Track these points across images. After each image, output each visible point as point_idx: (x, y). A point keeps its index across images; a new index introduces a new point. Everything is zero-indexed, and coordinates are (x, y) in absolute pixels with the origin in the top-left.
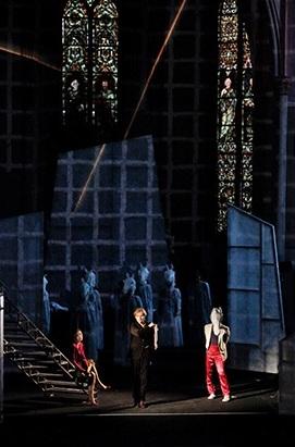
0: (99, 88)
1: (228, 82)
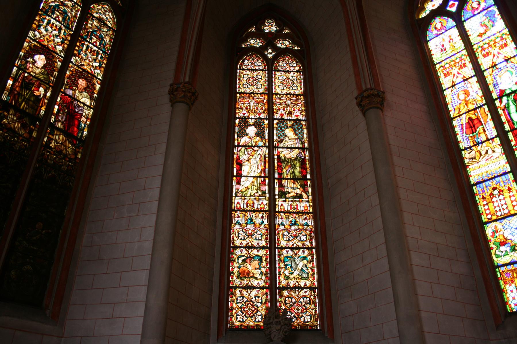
0: (73, 84)
1: (251, 131)
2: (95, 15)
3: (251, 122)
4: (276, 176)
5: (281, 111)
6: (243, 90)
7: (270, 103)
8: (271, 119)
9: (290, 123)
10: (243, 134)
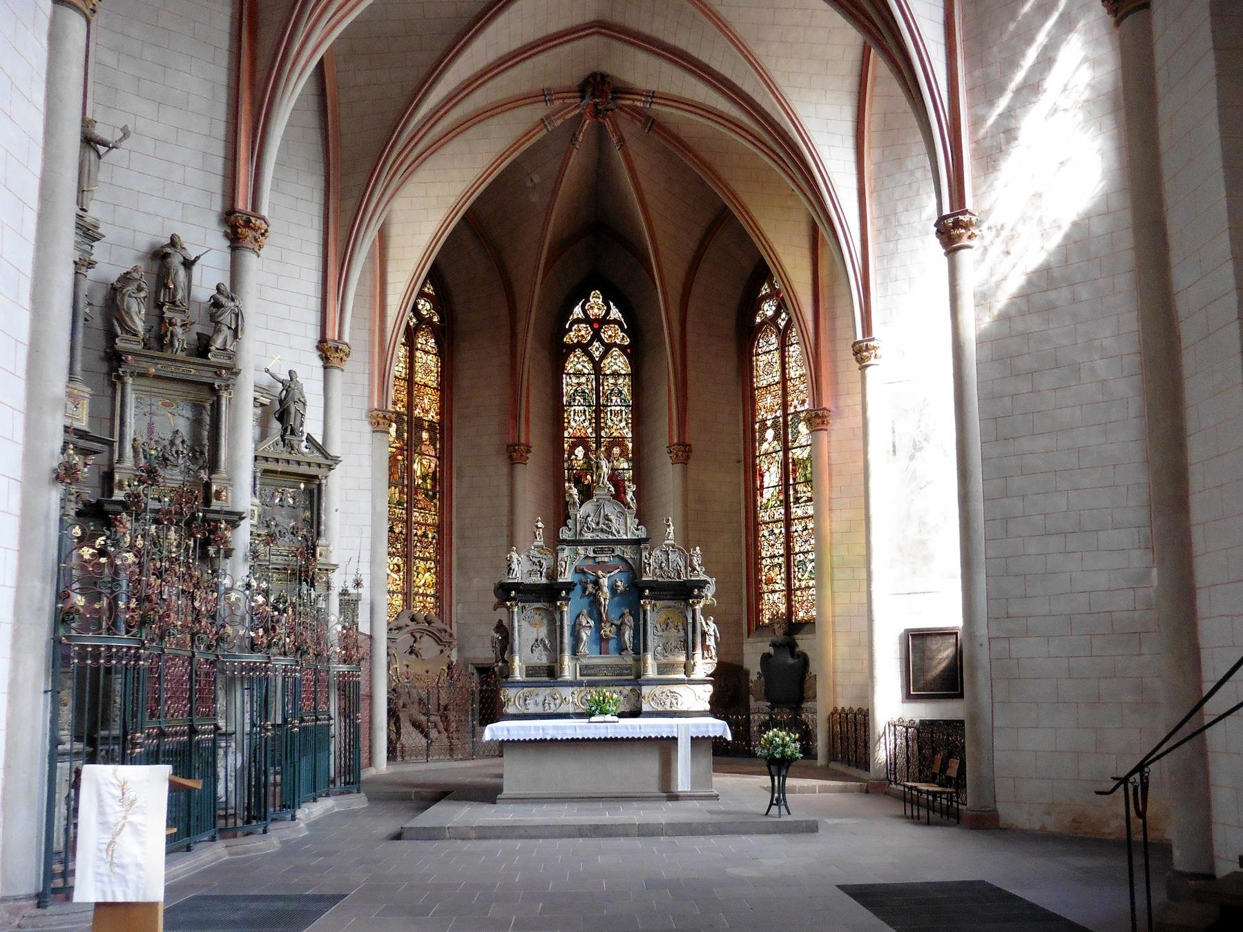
1: (770, 434)
2: (608, 372)
3: (769, 423)
4: (791, 482)
5: (796, 402)
8: (785, 415)
9: (802, 415)
10: (763, 440)
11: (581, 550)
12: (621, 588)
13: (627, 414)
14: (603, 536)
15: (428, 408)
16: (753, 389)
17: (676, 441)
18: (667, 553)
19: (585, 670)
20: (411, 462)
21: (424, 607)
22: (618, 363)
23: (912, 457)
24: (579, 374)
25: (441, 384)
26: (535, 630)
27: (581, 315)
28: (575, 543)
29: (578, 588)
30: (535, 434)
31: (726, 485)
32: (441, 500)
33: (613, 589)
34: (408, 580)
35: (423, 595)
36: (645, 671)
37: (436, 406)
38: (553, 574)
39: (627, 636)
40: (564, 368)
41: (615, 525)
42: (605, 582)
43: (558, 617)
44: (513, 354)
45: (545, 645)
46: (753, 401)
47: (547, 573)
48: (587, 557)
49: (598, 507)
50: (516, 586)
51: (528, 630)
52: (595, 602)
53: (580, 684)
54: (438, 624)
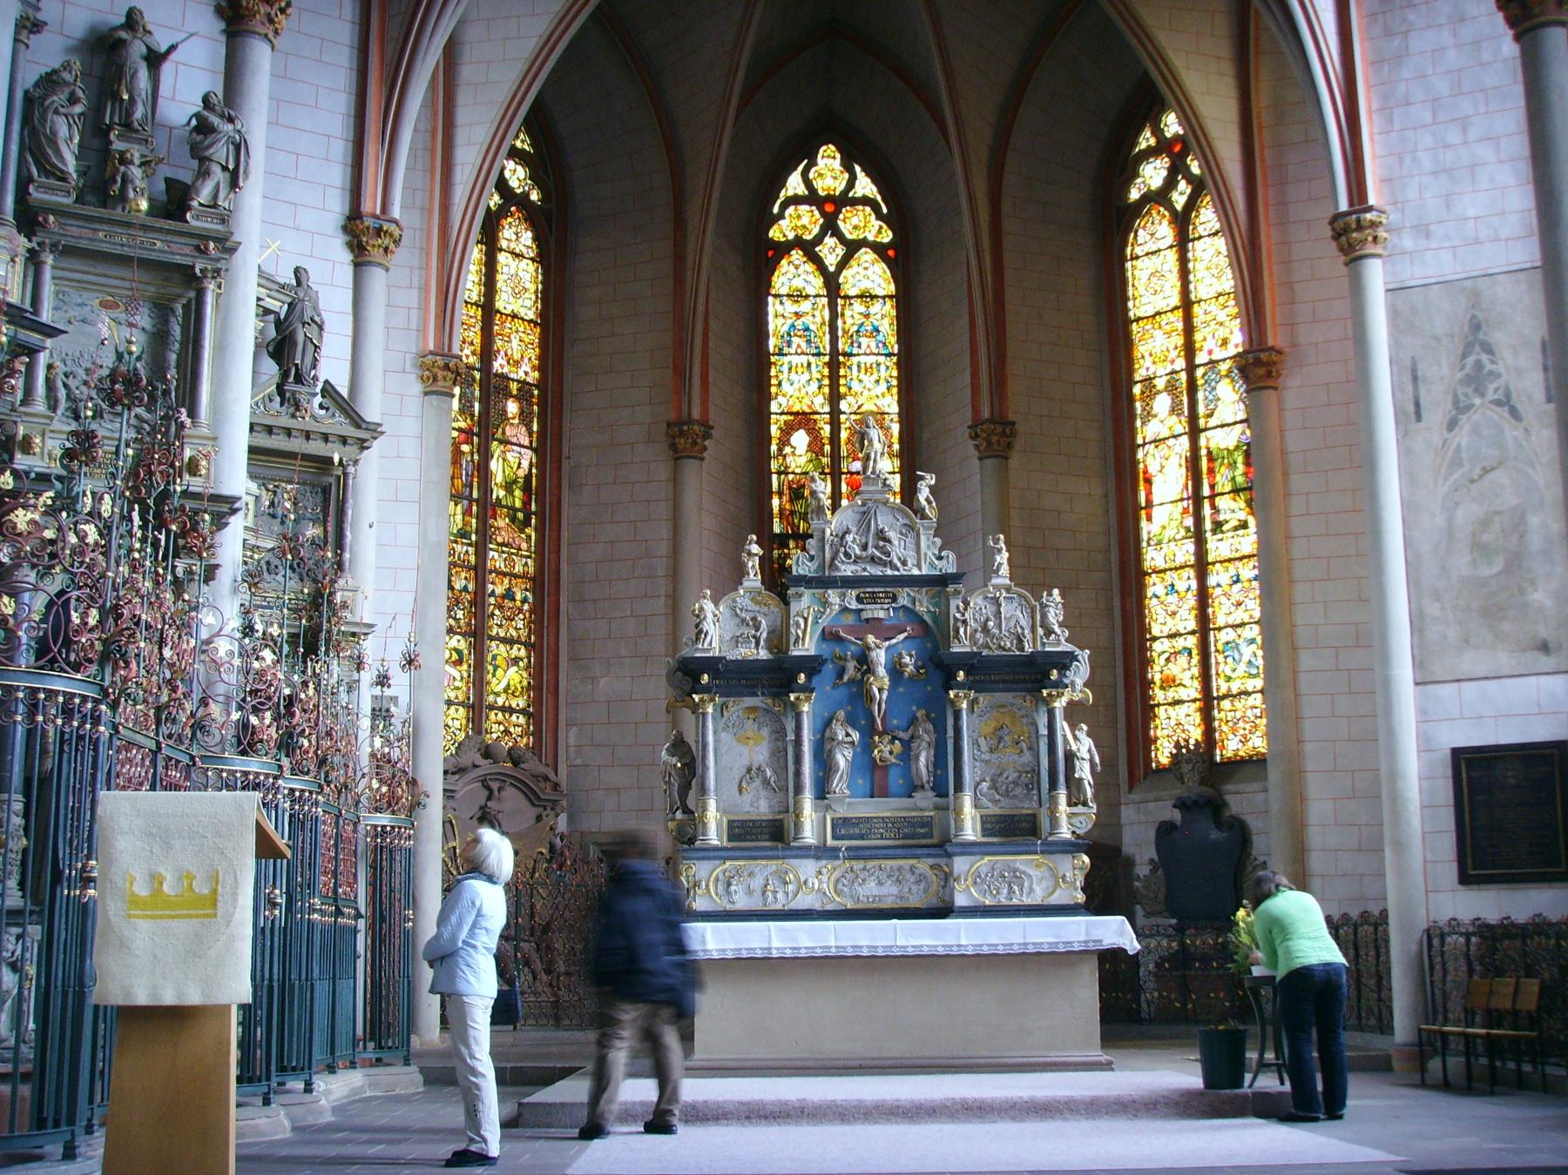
2: (852, 293)
6: (1140, 314)
7: (1189, 330)
11: (833, 596)
12: (910, 669)
13: (889, 370)
14: (876, 571)
15: (519, 355)
16: (1127, 322)
17: (986, 414)
18: (996, 601)
19: (842, 826)
20: (486, 456)
21: (507, 732)
22: (870, 275)
23: (1452, 425)
24: (797, 296)
25: (543, 314)
26: (746, 751)
27: (802, 190)
28: (822, 582)
29: (829, 668)
30: (721, 407)
31: (1084, 502)
32: (540, 530)
33: (895, 670)
34: (479, 681)
35: (503, 709)
36: (959, 828)
37: (533, 353)
38: (779, 639)
39: (922, 760)
40: (769, 285)
41: (899, 547)
42: (880, 657)
43: (790, 725)
44: (679, 258)
45: (766, 782)
46: (1128, 343)
47: (768, 640)
48: (845, 609)
49: (865, 517)
50: (713, 665)
51: (731, 747)
52: (860, 694)
53: (832, 853)
54: (532, 764)
